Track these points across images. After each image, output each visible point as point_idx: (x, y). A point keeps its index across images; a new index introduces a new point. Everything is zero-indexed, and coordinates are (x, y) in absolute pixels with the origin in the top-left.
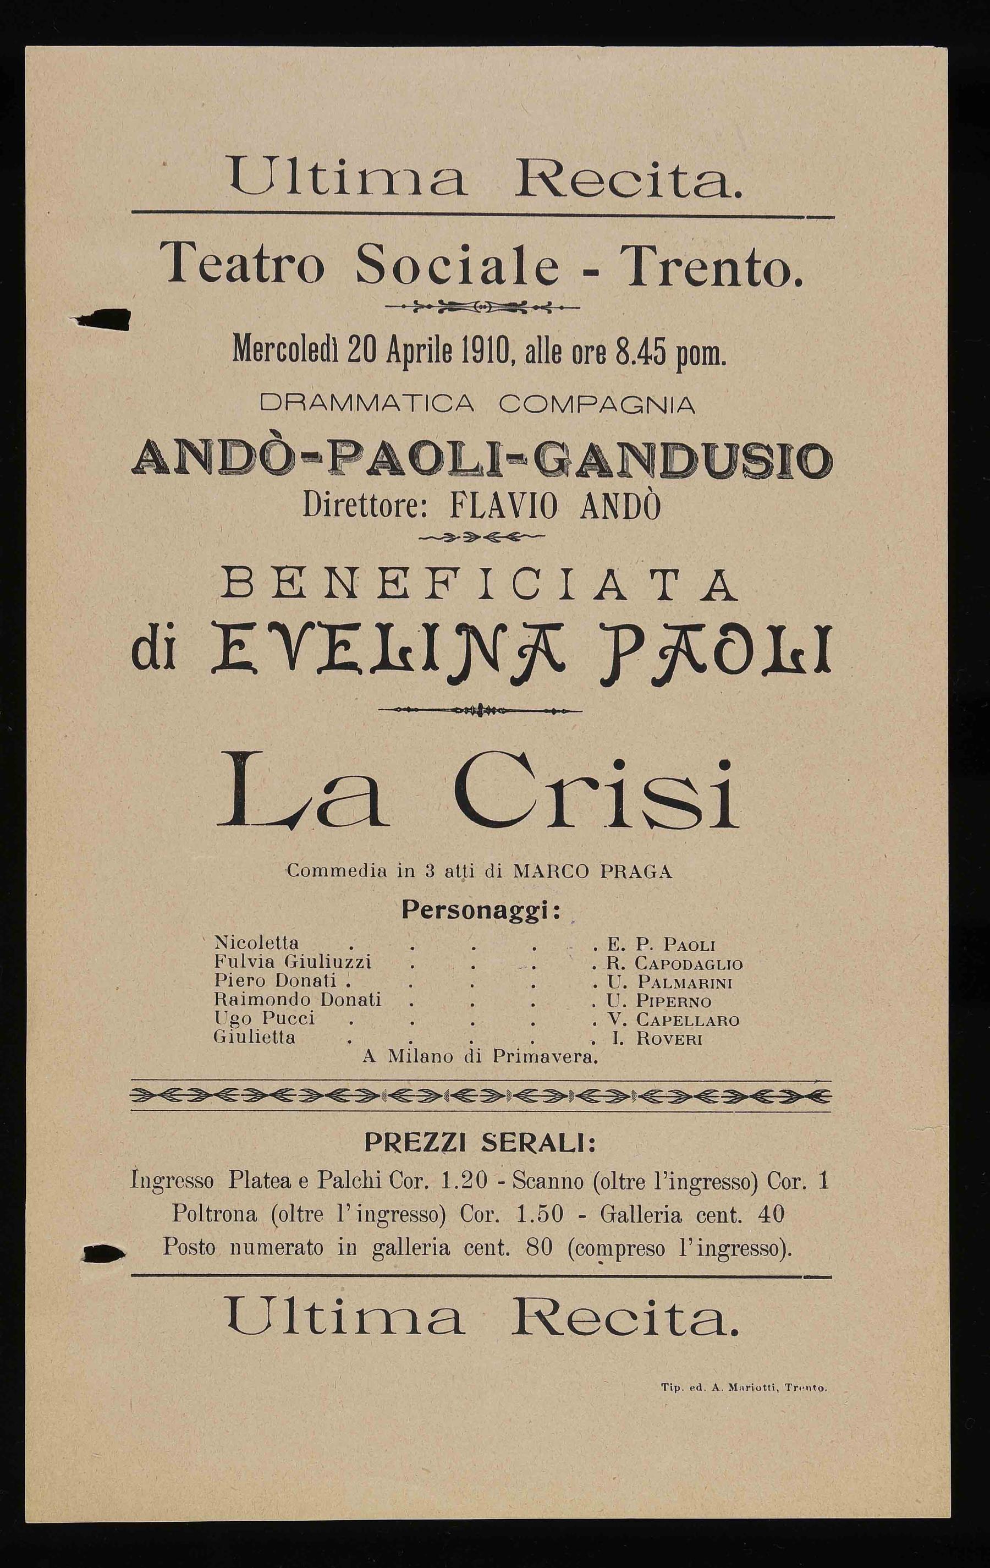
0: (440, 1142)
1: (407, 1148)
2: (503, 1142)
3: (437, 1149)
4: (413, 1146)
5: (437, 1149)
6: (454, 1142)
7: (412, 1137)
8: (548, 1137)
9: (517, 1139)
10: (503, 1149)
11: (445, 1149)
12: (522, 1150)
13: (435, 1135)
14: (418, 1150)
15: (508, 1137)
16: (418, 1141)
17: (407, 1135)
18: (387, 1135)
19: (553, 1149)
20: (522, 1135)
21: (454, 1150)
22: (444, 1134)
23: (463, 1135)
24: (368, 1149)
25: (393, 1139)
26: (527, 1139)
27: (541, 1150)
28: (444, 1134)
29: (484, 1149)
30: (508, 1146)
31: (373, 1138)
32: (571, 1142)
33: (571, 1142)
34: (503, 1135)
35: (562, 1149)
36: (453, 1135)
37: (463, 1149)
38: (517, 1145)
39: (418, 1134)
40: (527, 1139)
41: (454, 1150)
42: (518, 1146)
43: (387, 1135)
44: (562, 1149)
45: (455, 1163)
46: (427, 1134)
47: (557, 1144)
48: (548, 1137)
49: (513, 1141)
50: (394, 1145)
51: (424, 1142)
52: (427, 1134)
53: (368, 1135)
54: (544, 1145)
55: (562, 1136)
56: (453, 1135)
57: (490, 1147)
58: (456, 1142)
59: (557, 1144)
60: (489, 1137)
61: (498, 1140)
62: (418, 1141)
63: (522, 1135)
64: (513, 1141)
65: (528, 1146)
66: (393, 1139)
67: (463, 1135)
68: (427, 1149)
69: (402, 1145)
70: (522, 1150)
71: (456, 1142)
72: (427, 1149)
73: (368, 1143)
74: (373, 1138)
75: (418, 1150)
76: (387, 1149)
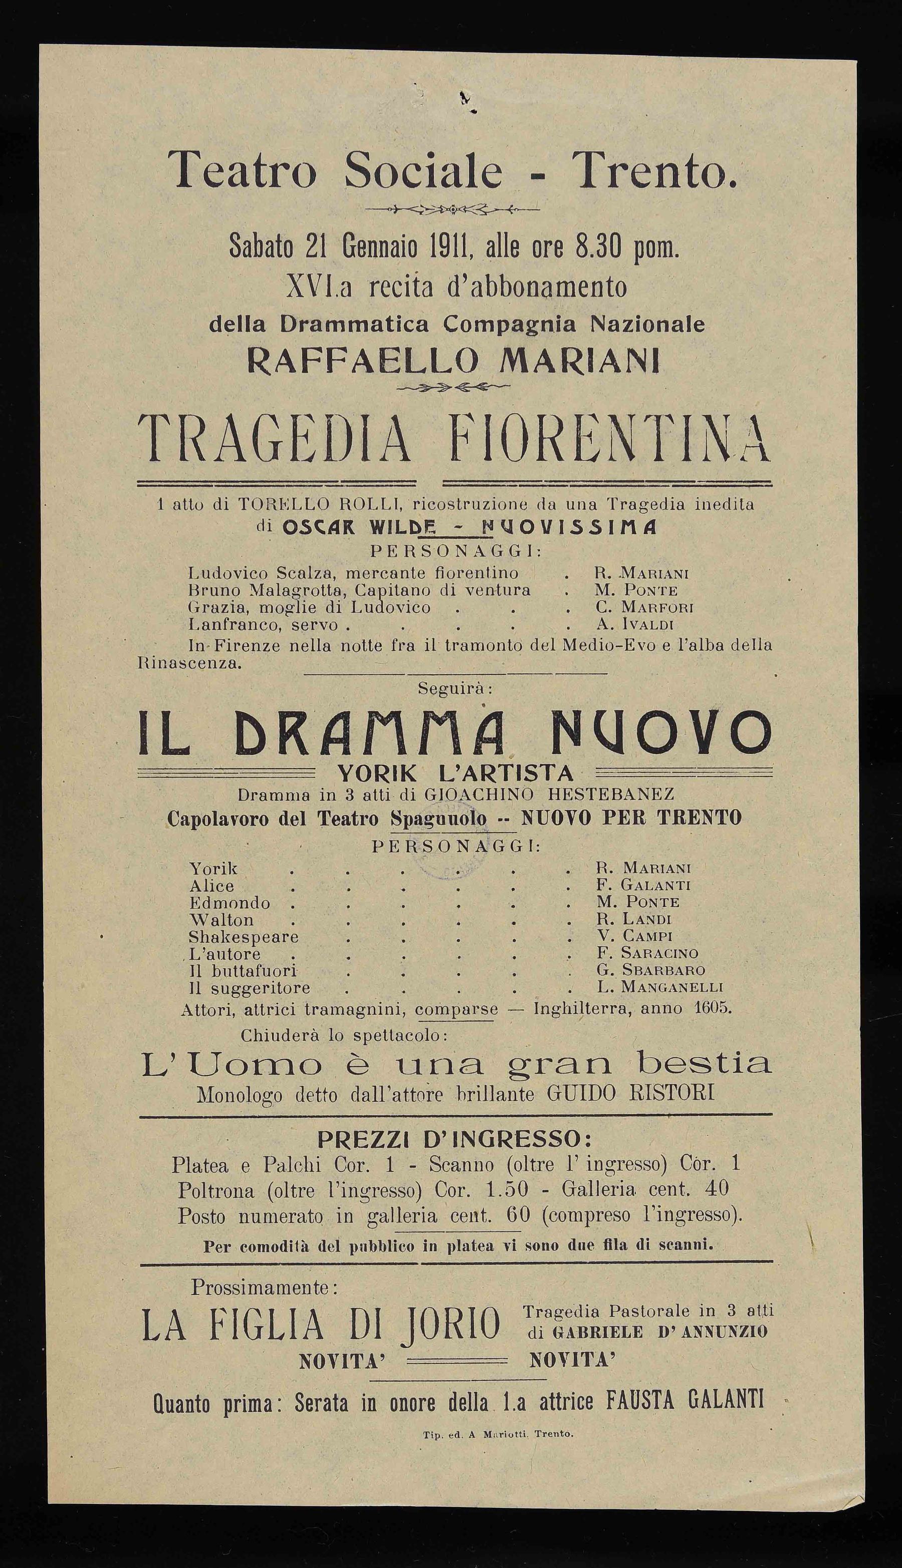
0: (386, 1139)
1: (356, 1145)
3: (383, 1146)
5: (383, 1146)
7: (360, 1135)
11: (390, 1146)
13: (381, 1133)
14: (366, 1146)
16: (365, 1139)
17: (356, 1133)
18: (338, 1133)
21: (399, 1146)
22: (389, 1132)
23: (406, 1134)
24: (321, 1146)
25: (343, 1137)
28: (389, 1132)
31: (325, 1136)
36: (397, 1133)
37: (406, 1146)
43: (338, 1133)
46: (373, 1132)
50: (343, 1142)
51: (371, 1138)
52: (373, 1132)
53: (321, 1133)
58: (400, 1140)
62: (365, 1139)
66: (343, 1137)
67: (406, 1134)
68: (374, 1146)
69: (351, 1142)
71: (400, 1140)
73: (321, 1141)
74: (325, 1136)
75: (366, 1146)
76: (338, 1146)
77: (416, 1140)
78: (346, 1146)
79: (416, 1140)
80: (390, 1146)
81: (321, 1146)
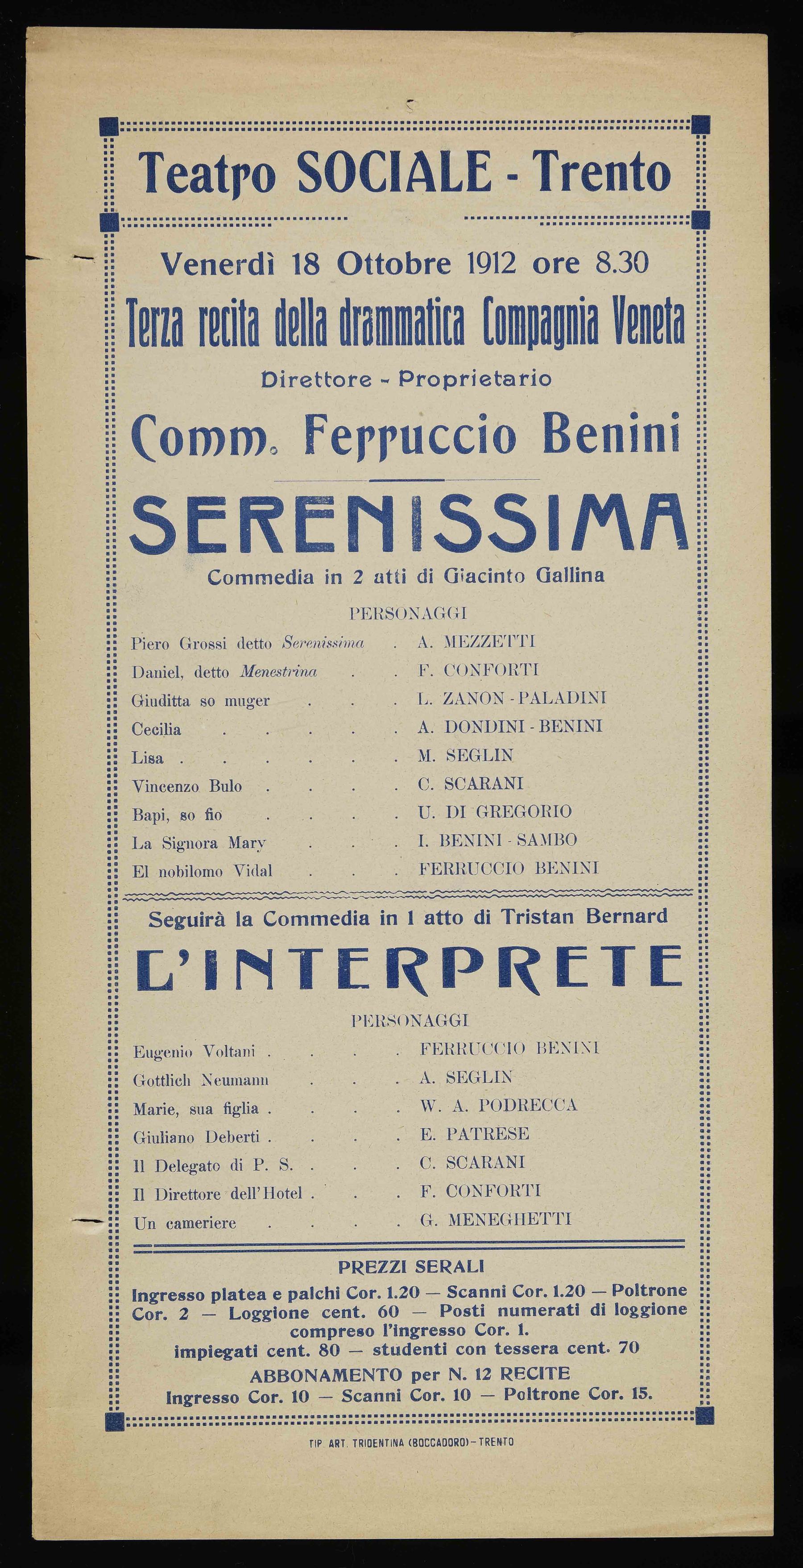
0: (389, 1267)
1: (368, 1271)
2: (429, 1266)
4: (371, 1270)
6: (399, 1267)
7: (371, 1264)
8: (459, 1263)
9: (439, 1265)
10: (429, 1271)
11: (392, 1271)
12: (442, 1271)
14: (375, 1272)
15: (432, 1263)
16: (374, 1267)
17: (368, 1262)
18: (354, 1263)
19: (463, 1271)
20: (442, 1262)
21: (399, 1272)
22: (392, 1262)
23: (404, 1262)
25: (358, 1265)
26: (446, 1264)
27: (455, 1271)
28: (392, 1262)
29: (417, 1271)
30: (433, 1269)
31: (344, 1265)
32: (475, 1266)
33: (475, 1266)
34: (429, 1262)
35: (469, 1270)
36: (398, 1262)
37: (404, 1271)
38: (439, 1268)
39: (375, 1262)
40: (446, 1264)
41: (399, 1272)
42: (439, 1270)
43: (354, 1263)
44: (469, 1270)
45: (397, 1281)
46: (380, 1262)
47: (465, 1267)
48: (459, 1263)
49: (436, 1266)
50: (358, 1269)
52: (380, 1262)
54: (457, 1268)
55: (469, 1262)
56: (398, 1262)
57: (421, 1270)
59: (465, 1267)
60: (420, 1263)
61: (426, 1265)
63: (442, 1262)
64: (436, 1266)
65: (446, 1268)
68: (380, 1271)
69: (363, 1270)
70: (442, 1271)
72: (380, 1271)
74: (344, 1265)
75: (375, 1272)
76: (354, 1272)
77: (411, 1267)
78: (360, 1272)
79: (411, 1267)
80: (392, 1271)
81: (341, 1272)
